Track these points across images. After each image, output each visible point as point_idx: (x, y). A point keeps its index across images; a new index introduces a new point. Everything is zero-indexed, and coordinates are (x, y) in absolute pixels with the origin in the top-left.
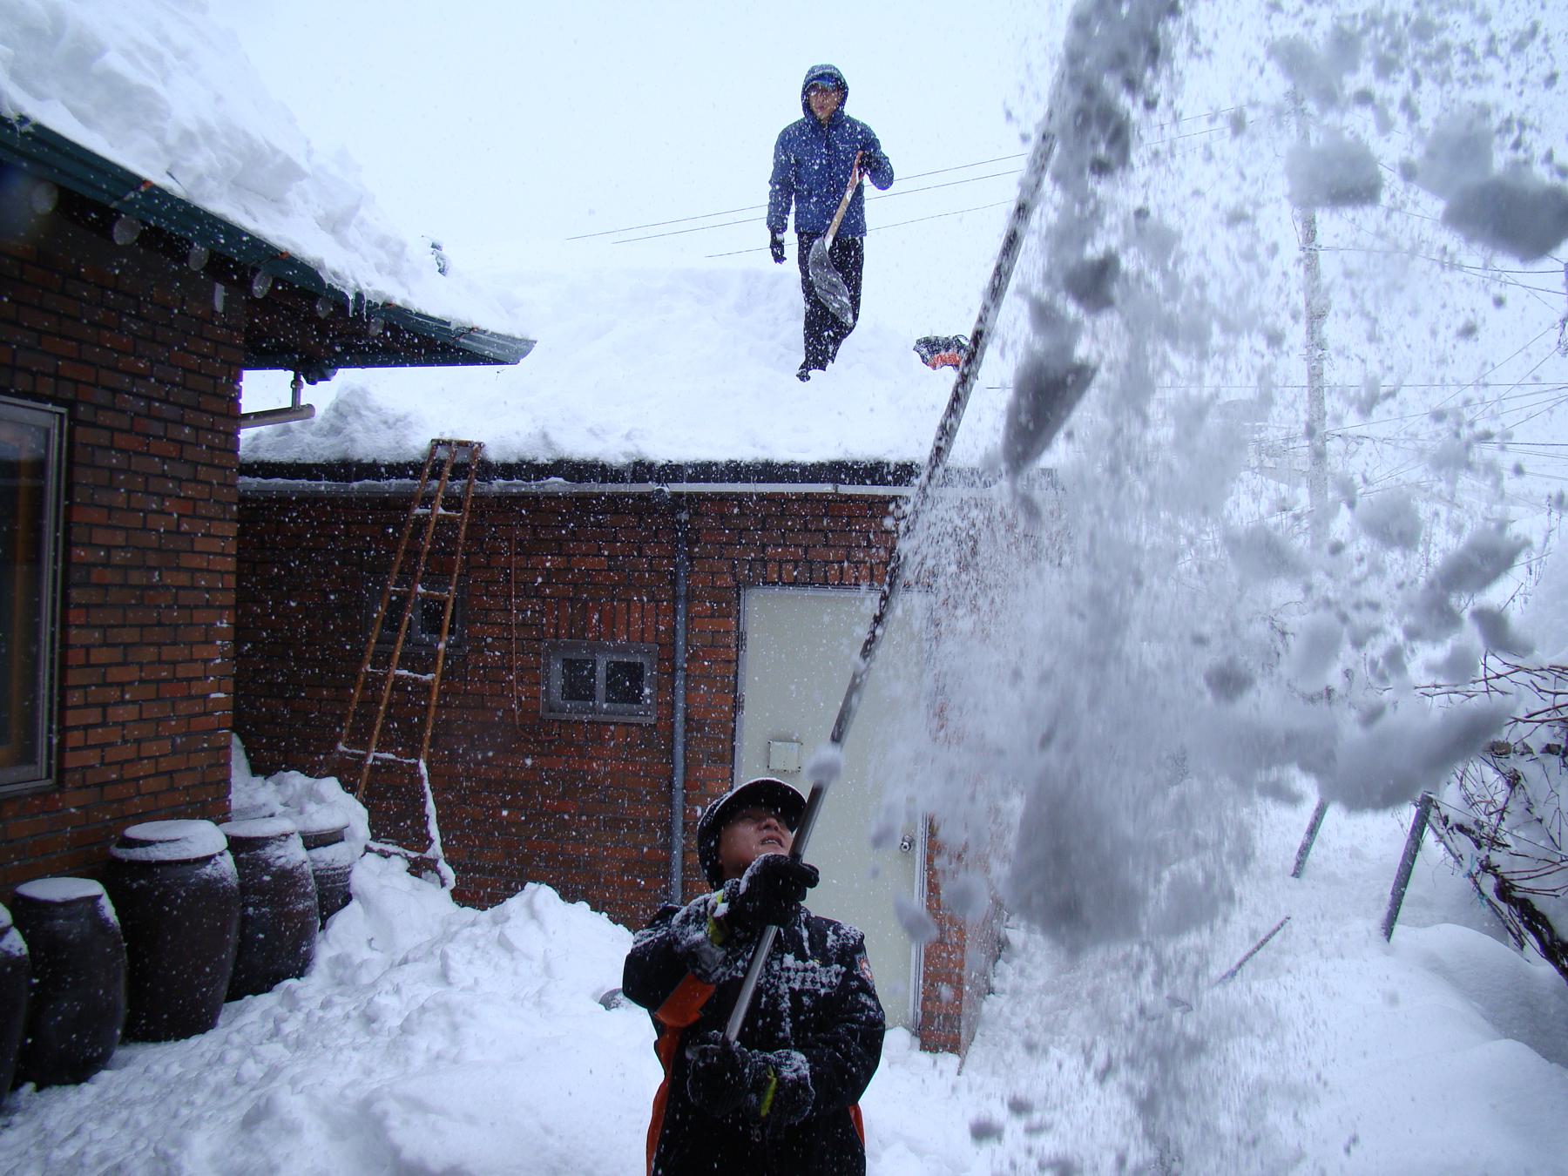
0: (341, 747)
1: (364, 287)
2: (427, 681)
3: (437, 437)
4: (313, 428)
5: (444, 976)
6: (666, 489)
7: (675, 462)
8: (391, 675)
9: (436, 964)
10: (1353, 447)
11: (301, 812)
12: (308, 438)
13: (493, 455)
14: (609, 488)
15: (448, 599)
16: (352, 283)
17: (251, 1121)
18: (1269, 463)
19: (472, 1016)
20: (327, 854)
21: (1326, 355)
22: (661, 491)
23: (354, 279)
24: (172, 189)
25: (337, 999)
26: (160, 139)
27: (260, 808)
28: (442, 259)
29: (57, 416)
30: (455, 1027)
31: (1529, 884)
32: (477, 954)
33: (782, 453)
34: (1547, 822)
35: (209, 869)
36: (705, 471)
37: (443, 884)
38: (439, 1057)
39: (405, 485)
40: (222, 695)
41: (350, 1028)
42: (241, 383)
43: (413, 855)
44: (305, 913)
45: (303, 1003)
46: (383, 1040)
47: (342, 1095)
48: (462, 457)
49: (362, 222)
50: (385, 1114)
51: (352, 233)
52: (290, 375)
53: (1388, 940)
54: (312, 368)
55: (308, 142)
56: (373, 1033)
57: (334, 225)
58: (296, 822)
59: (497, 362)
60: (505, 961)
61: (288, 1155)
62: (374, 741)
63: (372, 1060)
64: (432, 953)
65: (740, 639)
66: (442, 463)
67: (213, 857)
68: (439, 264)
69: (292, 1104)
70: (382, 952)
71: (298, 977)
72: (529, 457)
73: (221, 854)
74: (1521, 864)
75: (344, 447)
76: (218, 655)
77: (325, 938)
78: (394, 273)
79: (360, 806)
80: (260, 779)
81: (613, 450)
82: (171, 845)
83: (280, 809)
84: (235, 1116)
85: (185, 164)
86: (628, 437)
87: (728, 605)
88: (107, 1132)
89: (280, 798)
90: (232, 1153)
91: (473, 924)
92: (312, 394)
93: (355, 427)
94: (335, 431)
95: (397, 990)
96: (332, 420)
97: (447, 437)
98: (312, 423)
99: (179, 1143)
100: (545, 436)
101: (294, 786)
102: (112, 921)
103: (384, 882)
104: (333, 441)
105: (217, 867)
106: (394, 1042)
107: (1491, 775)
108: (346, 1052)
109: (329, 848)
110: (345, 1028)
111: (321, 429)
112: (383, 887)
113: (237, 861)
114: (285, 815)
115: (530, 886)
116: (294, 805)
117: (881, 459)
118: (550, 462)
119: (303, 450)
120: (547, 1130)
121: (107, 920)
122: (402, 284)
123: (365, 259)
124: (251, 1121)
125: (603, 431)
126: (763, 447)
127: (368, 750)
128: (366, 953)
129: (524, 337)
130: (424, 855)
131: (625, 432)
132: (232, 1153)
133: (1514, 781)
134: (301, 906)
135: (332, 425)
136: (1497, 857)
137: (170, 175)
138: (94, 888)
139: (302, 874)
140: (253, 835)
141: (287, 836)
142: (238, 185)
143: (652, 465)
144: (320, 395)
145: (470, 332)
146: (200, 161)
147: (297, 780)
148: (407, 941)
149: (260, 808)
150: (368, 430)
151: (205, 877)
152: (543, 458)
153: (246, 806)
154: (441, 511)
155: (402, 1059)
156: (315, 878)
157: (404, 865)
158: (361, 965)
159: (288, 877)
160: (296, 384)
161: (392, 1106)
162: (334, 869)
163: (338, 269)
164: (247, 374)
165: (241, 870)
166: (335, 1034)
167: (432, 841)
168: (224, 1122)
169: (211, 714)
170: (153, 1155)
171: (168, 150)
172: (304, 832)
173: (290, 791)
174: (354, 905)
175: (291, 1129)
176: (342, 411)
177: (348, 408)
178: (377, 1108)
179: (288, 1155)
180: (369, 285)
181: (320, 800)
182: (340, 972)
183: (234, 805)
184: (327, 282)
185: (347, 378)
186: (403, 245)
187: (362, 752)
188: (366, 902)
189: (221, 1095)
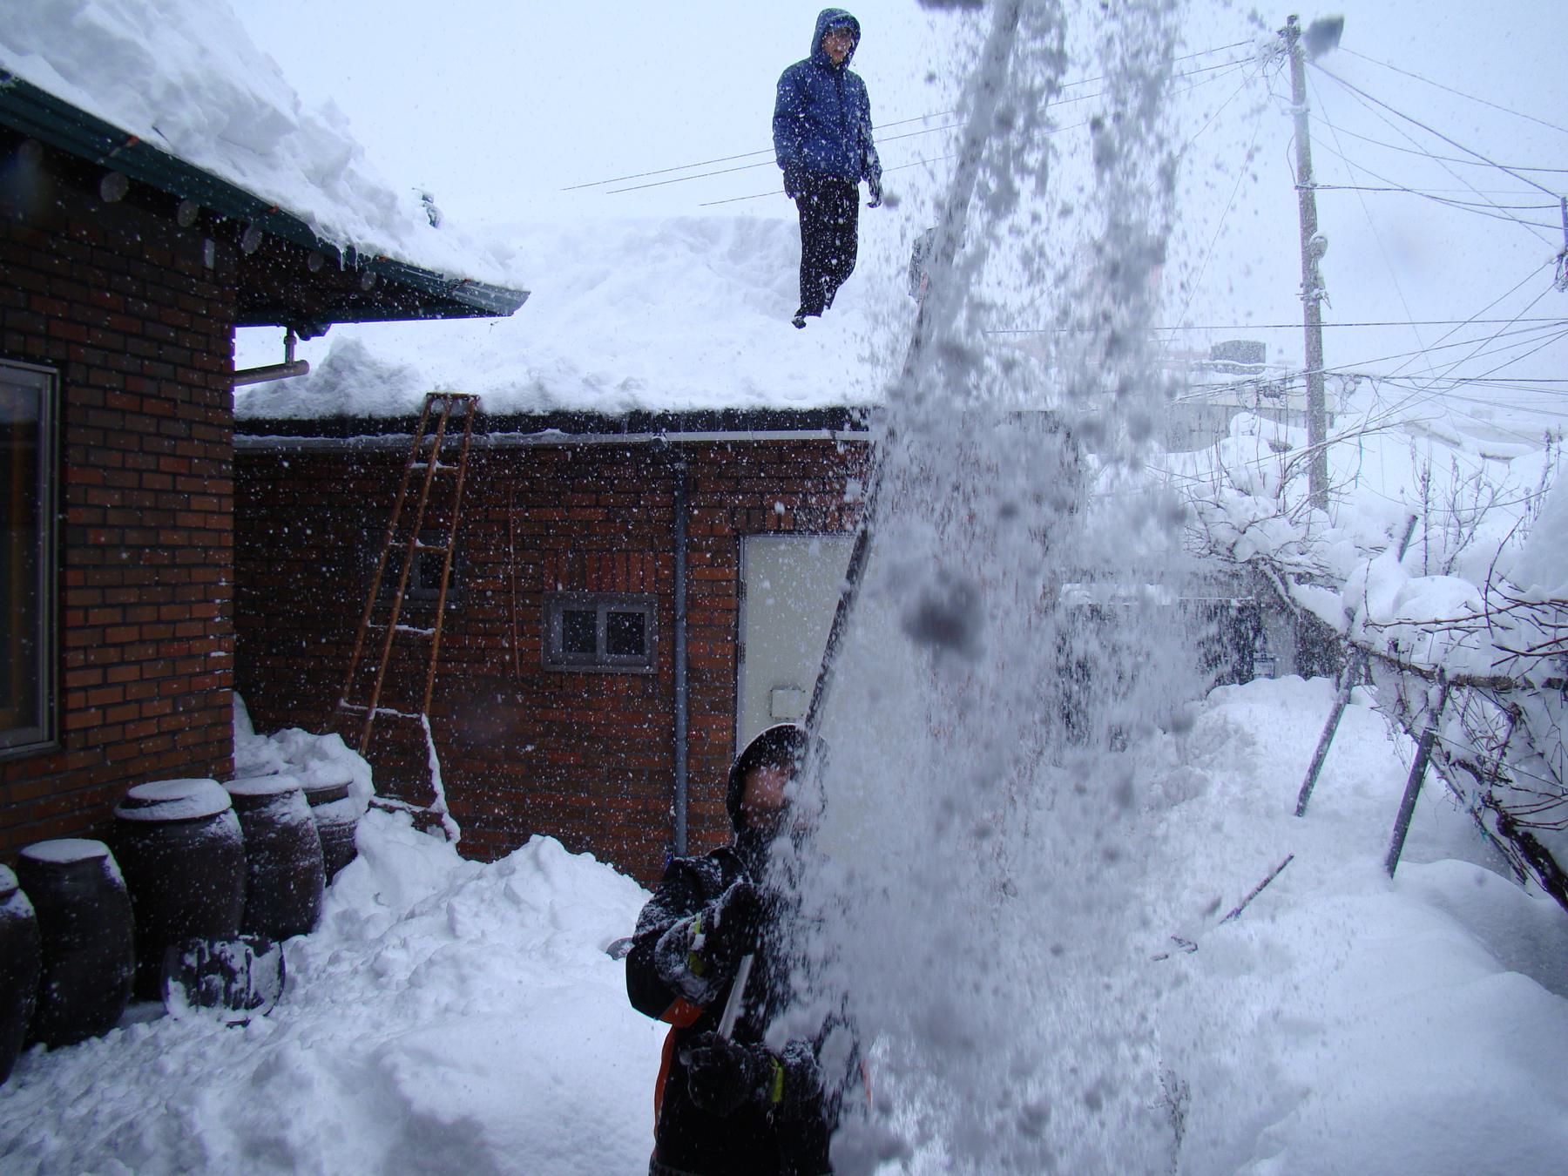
0: (343, 703)
1: (355, 240)
2: (428, 636)
3: (432, 390)
4: (308, 384)
5: (451, 929)
8: (392, 631)
9: (443, 918)
10: (1351, 386)
11: (305, 769)
12: (303, 394)
13: (489, 407)
15: (447, 553)
16: (342, 237)
17: (262, 1077)
18: (1266, 402)
19: (479, 968)
20: (331, 811)
21: (1323, 295)
22: (658, 441)
23: (346, 233)
24: (158, 145)
25: (345, 954)
26: (145, 93)
27: (264, 766)
28: (433, 211)
29: (49, 377)
30: (463, 979)
31: (1531, 818)
32: (483, 907)
33: (779, 401)
34: (1548, 756)
35: (213, 827)
36: (707, 420)
37: (448, 838)
38: (447, 1009)
39: (400, 440)
40: (222, 654)
41: (359, 982)
42: (234, 340)
43: (418, 809)
44: (312, 869)
45: (311, 959)
46: (391, 994)
47: (351, 1049)
48: (458, 410)
49: (352, 174)
50: (395, 1067)
51: (342, 186)
52: (283, 331)
53: (1392, 877)
54: (306, 323)
55: (295, 95)
56: (382, 988)
57: (324, 178)
58: (299, 779)
59: (492, 314)
60: (511, 913)
61: (299, 1110)
62: (376, 696)
63: (380, 1015)
64: (439, 907)
65: (740, 590)
66: (439, 416)
67: (217, 815)
68: (430, 216)
69: (301, 1058)
70: (388, 906)
71: (306, 935)
72: (525, 409)
73: (225, 812)
74: (1522, 799)
75: (339, 403)
76: (218, 611)
77: (332, 894)
78: (385, 225)
79: (363, 761)
80: (262, 737)
81: (609, 400)
82: (175, 805)
83: (285, 766)
84: (245, 1072)
85: (170, 118)
86: (624, 386)
87: (729, 550)
88: (120, 1090)
89: (283, 756)
90: (243, 1109)
91: (480, 877)
92: (305, 350)
93: (350, 383)
94: (330, 386)
95: (404, 944)
96: (327, 376)
97: (442, 390)
98: (307, 379)
99: (190, 1099)
100: (540, 388)
101: (297, 743)
102: (118, 881)
103: (390, 837)
104: (328, 396)
105: (222, 825)
106: (402, 996)
107: (1492, 711)
108: (354, 1007)
109: (334, 804)
110: (354, 983)
111: (316, 385)
112: (388, 842)
113: (241, 818)
114: (287, 772)
115: (535, 838)
116: (297, 762)
118: (547, 414)
119: (298, 407)
120: (557, 1080)
121: (113, 880)
122: (394, 237)
123: (355, 212)
124: (262, 1077)
125: (599, 381)
126: (760, 395)
127: (370, 706)
128: (372, 909)
130: (429, 810)
131: (621, 381)
132: (243, 1109)
133: (1515, 716)
134: (307, 862)
135: (326, 382)
136: (1499, 793)
137: (157, 130)
138: (99, 849)
139: (307, 830)
140: (258, 792)
141: (291, 793)
142: (225, 140)
143: (649, 414)
144: (314, 351)
145: (464, 284)
146: (187, 115)
147: (299, 738)
148: (415, 894)
149: (264, 766)
150: (363, 385)
151: (210, 835)
152: (539, 410)
153: (249, 763)
154: (438, 465)
155: (410, 1012)
156: (321, 834)
157: (408, 819)
158: (368, 921)
159: (292, 834)
160: (289, 342)
161: (402, 1060)
162: (339, 825)
163: (328, 223)
164: (239, 331)
165: (246, 828)
166: (343, 989)
167: (434, 795)
168: (236, 1078)
169: (211, 672)
170: (166, 1112)
171: (154, 105)
172: (308, 789)
173: (293, 748)
174: (360, 861)
175: (301, 1084)
176: (335, 367)
177: (342, 363)
178: (387, 1061)
179: (299, 1110)
180: (360, 238)
181: (323, 756)
182: (347, 927)
183: (237, 764)
184: (318, 236)
185: (340, 332)
186: (393, 198)
187: (365, 708)
188: (372, 858)
189: (232, 1052)
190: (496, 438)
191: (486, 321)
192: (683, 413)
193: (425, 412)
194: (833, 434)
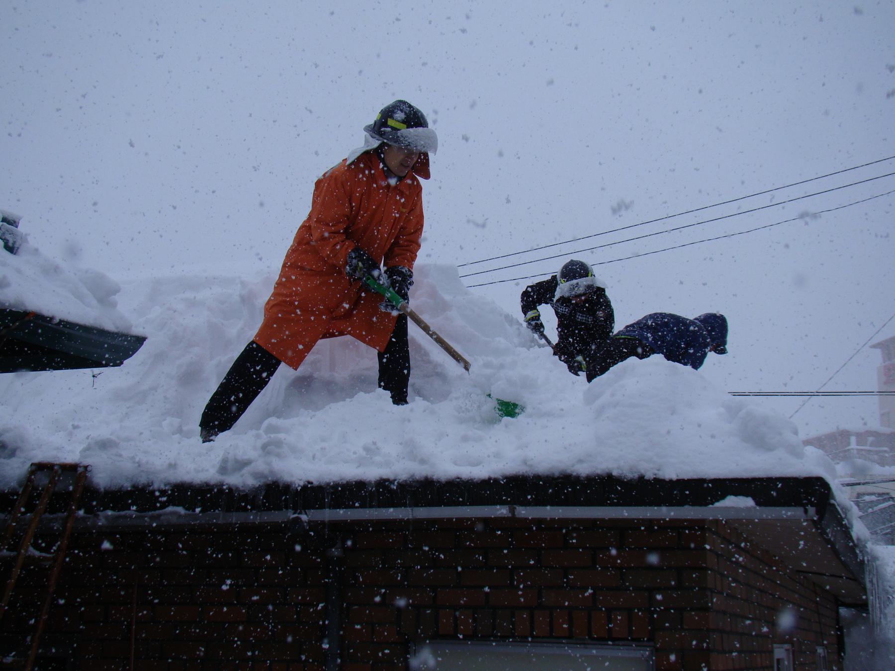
6: (304, 517)
7: (316, 483)
13: (101, 479)
14: (235, 518)
22: (298, 519)
72: (143, 480)
117: (569, 471)
126: (423, 461)
129: (125, 331)
190: (107, 517)
191: (84, 374)
192: (328, 484)
193: (26, 486)
194: (512, 511)
